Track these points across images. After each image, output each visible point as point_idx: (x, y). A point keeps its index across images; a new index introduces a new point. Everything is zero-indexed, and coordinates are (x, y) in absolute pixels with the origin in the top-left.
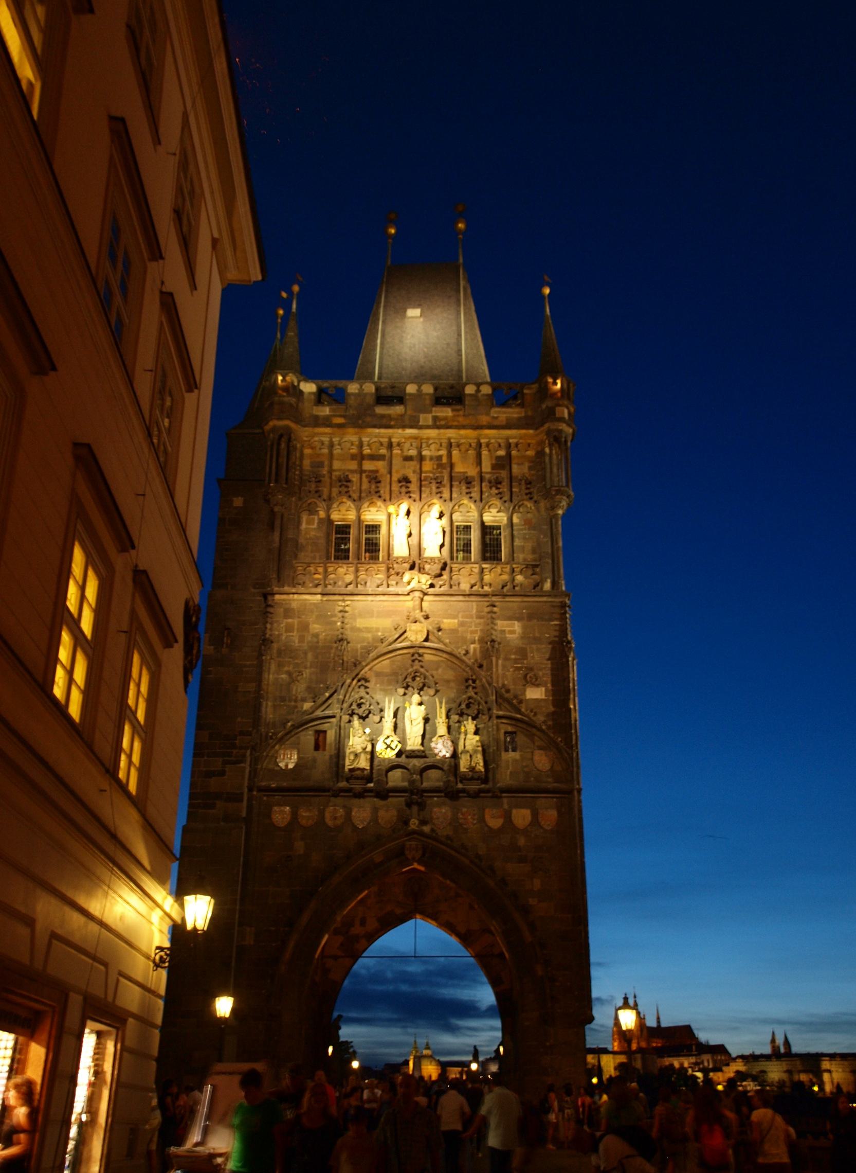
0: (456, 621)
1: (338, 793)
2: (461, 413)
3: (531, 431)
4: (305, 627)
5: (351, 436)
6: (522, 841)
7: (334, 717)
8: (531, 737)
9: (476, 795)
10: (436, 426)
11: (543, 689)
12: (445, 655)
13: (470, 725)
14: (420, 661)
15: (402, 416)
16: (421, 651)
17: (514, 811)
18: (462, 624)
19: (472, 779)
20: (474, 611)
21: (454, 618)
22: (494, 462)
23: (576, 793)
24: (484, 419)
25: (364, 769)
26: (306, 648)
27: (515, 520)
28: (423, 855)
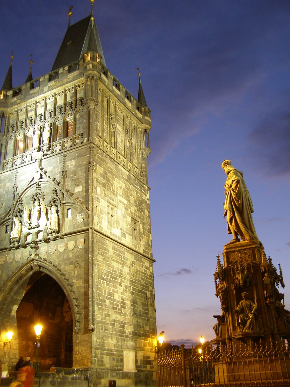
0: (52, 167)
1: (11, 249)
2: (58, 81)
3: (82, 78)
4: (5, 185)
5: (23, 105)
6: (71, 256)
7: (10, 219)
8: (76, 209)
9: (55, 239)
10: (49, 90)
11: (82, 186)
12: (47, 183)
13: (54, 209)
14: (39, 188)
15: (38, 91)
16: (40, 183)
17: (69, 243)
18: (54, 168)
19: (51, 233)
20: (59, 160)
21: (52, 166)
22: (71, 96)
23: (90, 230)
24: (65, 80)
25: (16, 238)
26: (5, 193)
27: (77, 117)
28: (40, 268)
